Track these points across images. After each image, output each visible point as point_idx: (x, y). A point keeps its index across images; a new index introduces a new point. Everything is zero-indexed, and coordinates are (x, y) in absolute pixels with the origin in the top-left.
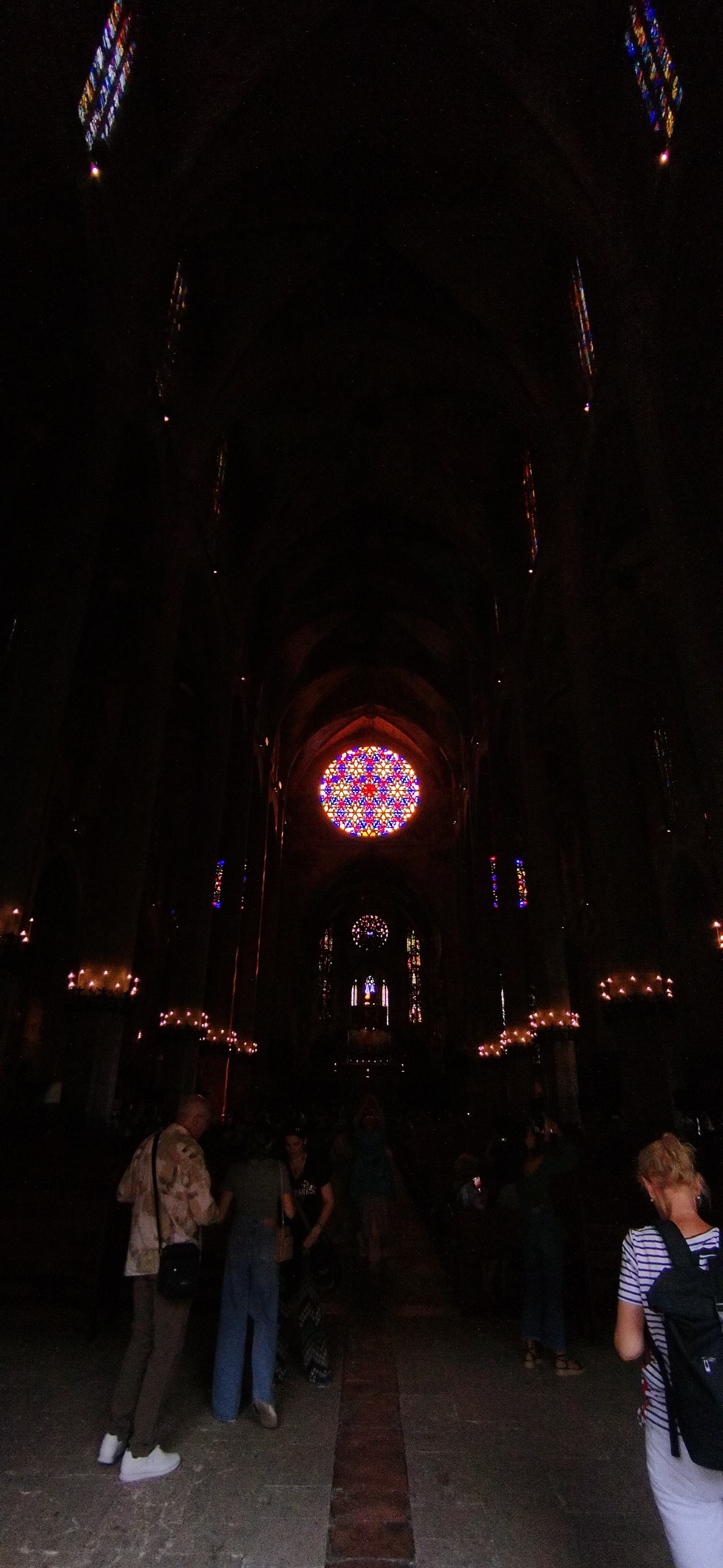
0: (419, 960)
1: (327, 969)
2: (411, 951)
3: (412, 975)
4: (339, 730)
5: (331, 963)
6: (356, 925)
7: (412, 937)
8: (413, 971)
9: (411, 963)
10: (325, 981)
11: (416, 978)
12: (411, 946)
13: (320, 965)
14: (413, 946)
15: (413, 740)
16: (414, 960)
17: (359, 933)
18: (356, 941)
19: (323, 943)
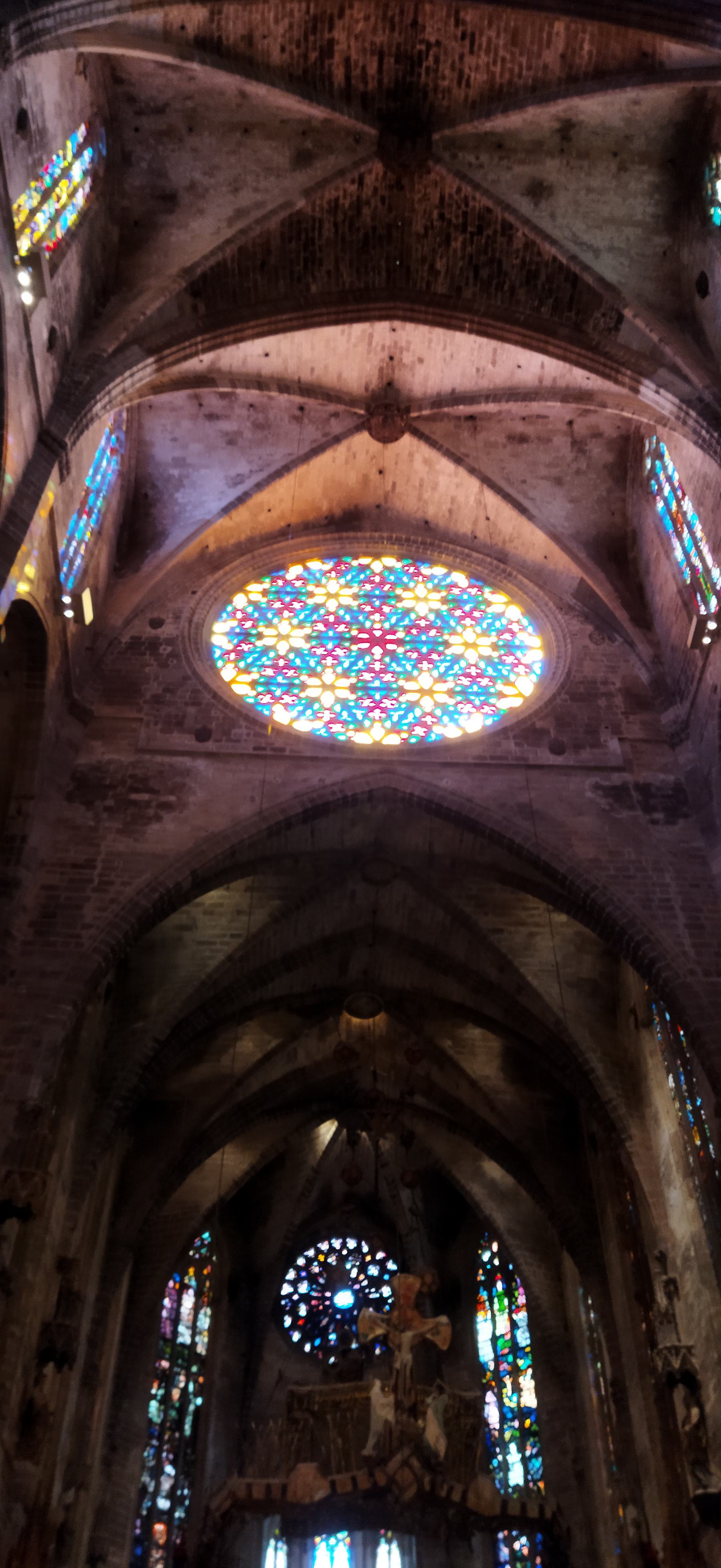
0: (532, 1384)
1: (179, 1425)
2: (497, 1360)
3: (505, 1452)
4: (286, 469)
5: (199, 1401)
6: (298, 1269)
7: (496, 1306)
8: (507, 1435)
9: (501, 1404)
10: (169, 1469)
11: (525, 1461)
12: (494, 1339)
13: (154, 1397)
14: (502, 1336)
15: (522, 510)
16: (508, 1390)
17: (305, 1298)
18: (294, 1327)
19: (176, 1319)
